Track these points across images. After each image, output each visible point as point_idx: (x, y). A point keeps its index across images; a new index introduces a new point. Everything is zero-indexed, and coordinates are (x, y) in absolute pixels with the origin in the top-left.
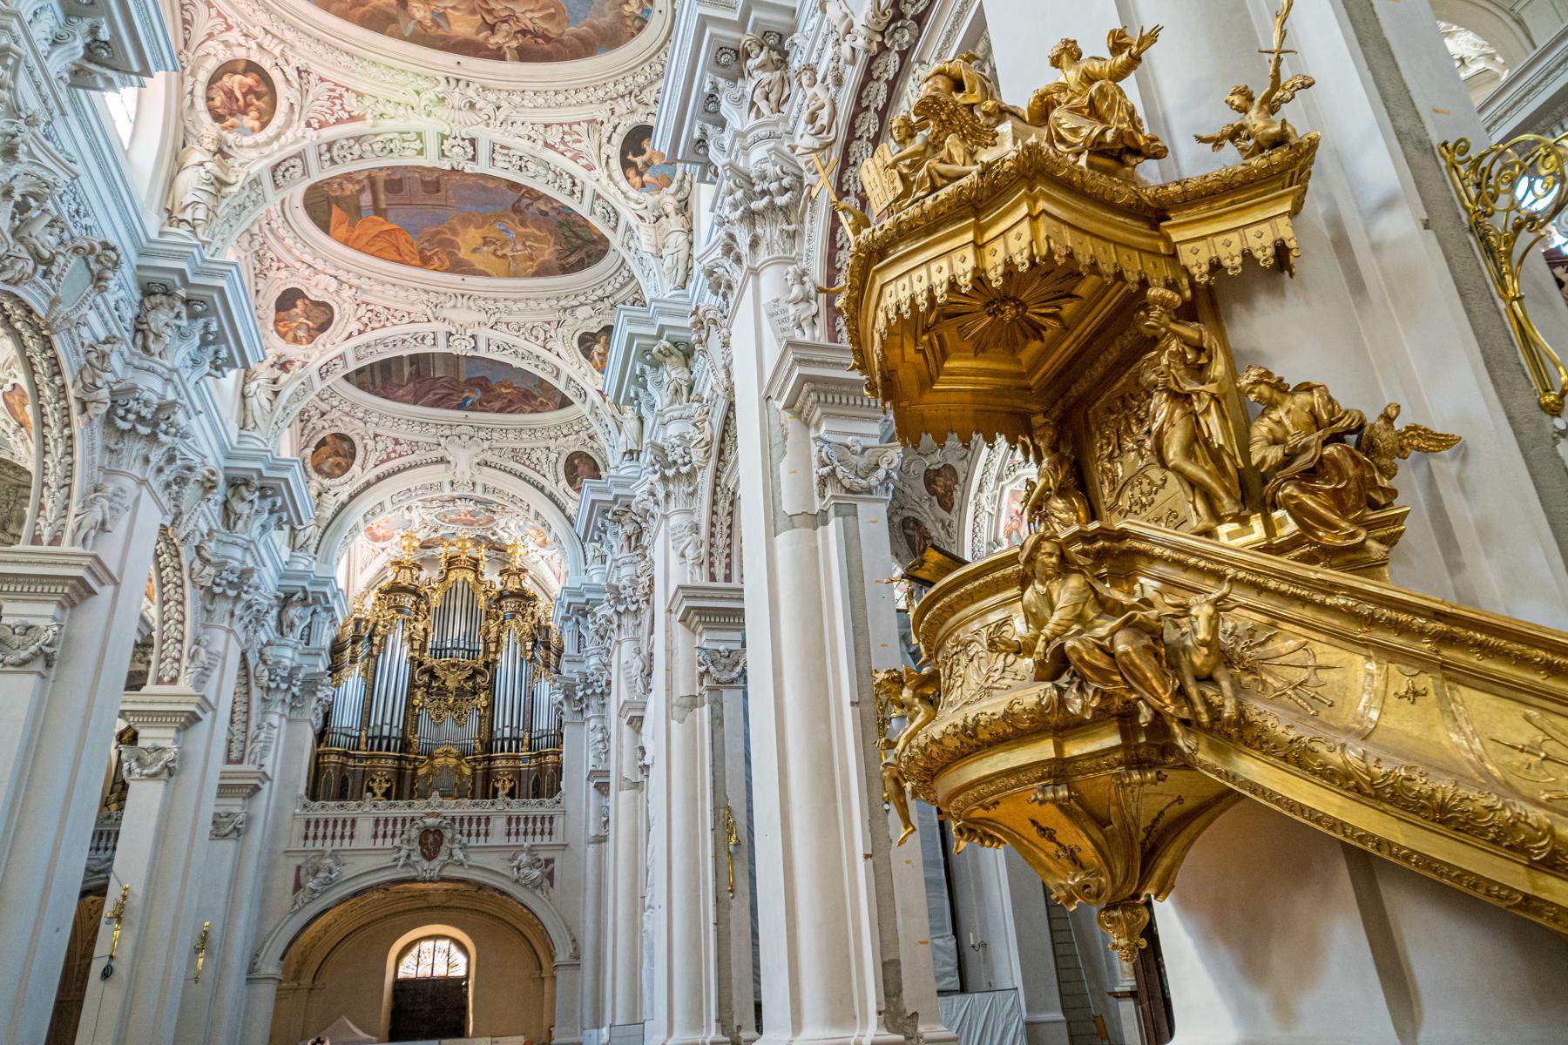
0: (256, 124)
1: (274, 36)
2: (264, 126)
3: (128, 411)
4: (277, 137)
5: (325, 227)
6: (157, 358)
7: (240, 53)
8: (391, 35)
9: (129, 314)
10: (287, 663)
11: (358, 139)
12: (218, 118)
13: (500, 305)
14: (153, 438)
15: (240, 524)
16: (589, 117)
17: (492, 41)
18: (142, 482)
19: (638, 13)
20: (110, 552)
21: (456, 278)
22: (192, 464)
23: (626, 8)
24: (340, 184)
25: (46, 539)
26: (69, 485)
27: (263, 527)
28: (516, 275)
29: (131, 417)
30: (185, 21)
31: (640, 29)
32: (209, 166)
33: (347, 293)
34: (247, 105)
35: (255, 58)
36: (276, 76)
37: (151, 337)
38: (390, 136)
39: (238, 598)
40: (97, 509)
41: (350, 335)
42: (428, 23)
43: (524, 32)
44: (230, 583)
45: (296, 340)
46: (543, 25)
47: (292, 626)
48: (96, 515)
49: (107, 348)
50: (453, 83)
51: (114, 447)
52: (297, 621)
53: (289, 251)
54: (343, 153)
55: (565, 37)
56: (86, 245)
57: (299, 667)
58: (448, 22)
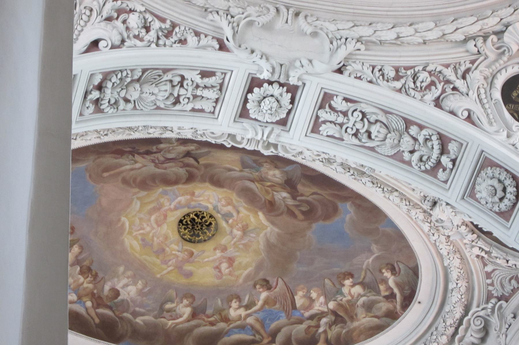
11: (398, 157)
38: (355, 141)
46: (121, 161)
54: (424, 151)
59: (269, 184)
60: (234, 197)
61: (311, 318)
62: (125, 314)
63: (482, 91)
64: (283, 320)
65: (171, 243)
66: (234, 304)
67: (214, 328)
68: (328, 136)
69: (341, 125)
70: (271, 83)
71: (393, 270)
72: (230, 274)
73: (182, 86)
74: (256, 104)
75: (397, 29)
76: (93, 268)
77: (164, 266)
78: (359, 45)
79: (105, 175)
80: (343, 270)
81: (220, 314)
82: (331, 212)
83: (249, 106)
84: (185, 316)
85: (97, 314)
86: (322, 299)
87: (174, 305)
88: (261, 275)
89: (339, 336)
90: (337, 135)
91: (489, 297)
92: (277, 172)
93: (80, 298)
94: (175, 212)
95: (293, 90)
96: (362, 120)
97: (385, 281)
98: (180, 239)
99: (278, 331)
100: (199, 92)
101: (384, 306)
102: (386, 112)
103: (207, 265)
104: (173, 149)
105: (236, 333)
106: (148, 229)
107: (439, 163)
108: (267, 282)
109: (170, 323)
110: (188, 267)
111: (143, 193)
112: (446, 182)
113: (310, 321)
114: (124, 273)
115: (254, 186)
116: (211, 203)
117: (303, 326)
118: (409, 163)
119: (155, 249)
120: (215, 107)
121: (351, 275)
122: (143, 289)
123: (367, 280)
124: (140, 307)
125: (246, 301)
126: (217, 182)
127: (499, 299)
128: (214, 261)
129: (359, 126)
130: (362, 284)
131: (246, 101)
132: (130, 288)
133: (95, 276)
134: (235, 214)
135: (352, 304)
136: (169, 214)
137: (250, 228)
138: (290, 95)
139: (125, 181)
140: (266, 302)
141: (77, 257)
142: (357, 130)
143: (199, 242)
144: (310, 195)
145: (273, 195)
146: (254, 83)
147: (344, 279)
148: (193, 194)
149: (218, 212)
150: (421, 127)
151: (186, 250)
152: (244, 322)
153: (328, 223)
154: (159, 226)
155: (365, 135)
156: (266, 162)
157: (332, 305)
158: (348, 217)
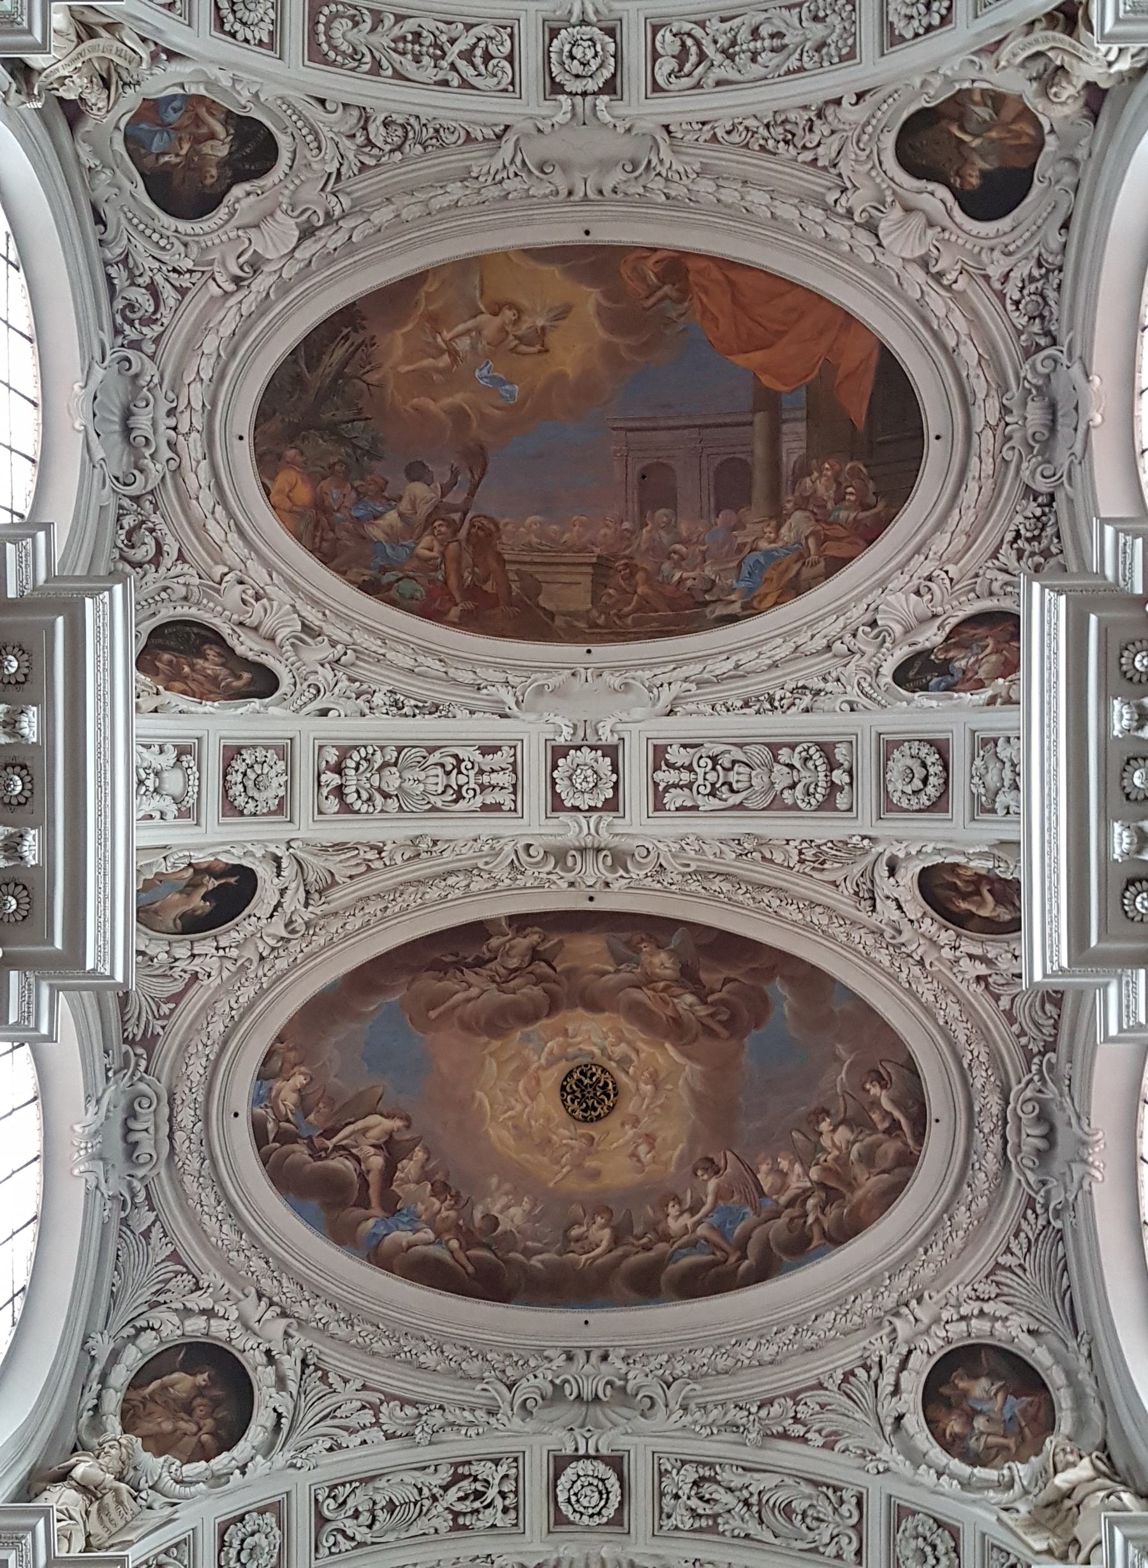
5: (889, 370)
11: (776, 804)
13: (495, 192)
16: (335, 894)
17: (536, 937)
19: (278, 1084)
21: (607, 234)
23: (299, 1080)
24: (840, 499)
28: (464, 266)
31: (270, 1055)
33: (859, 201)
35: (946, 937)
36: (915, 906)
38: (715, 803)
41: (860, 96)
42: (646, 948)
43: (481, 963)
45: (996, 99)
53: (975, 319)
55: (404, 979)
58: (613, 953)
59: (661, 985)
61: (790, 1204)
62: (512, 1255)
63: (865, 685)
64: (751, 1218)
65: (558, 1126)
66: (673, 1210)
67: (652, 1254)
68: (677, 809)
69: (689, 786)
70: (578, 748)
72: (654, 1160)
73: (460, 772)
74: (567, 782)
75: (735, 658)
76: (450, 1183)
77: (557, 1168)
78: (686, 686)
79: (433, 1014)
80: (812, 1107)
81: (655, 1230)
82: (761, 1007)
83: (558, 789)
84: (604, 1245)
85: (468, 1258)
86: (798, 1168)
87: (584, 1228)
88: (699, 1153)
89: (839, 1219)
90: (689, 804)
92: (662, 957)
93: (438, 1235)
94: (550, 1072)
95: (611, 752)
96: (714, 769)
97: (876, 1103)
98: (570, 1119)
99: (746, 1237)
100: (486, 779)
101: (890, 1148)
102: (740, 746)
104: (512, 947)
105: (685, 1255)
106: (519, 1107)
107: (833, 787)
108: (711, 1161)
109: (584, 1257)
110: (591, 1163)
111: (496, 1044)
112: (850, 810)
113: (789, 1210)
114: (498, 1188)
116: (595, 1044)
117: (783, 1220)
118: (795, 807)
119: (537, 1140)
120: (515, 801)
122: (533, 1209)
123: (850, 1113)
124: (533, 1240)
125: (688, 1202)
126: (593, 1005)
127: (1042, 1054)
128: (626, 1144)
129: (712, 777)
131: (554, 783)
132: (512, 1210)
133: (457, 1197)
134: (634, 1056)
135: (843, 1160)
136: (543, 1075)
137: (662, 1076)
138: (608, 760)
139: (466, 1026)
140: (718, 1196)
141: (423, 1167)
142: (713, 785)
143: (599, 1117)
144: (723, 985)
145: (674, 1005)
146: (559, 752)
147: (818, 1123)
148: (565, 1033)
149: (610, 1059)
150: (793, 747)
151: (583, 1135)
152: (693, 1236)
153: (761, 1031)
154: (532, 1099)
155: (725, 789)
156: (642, 940)
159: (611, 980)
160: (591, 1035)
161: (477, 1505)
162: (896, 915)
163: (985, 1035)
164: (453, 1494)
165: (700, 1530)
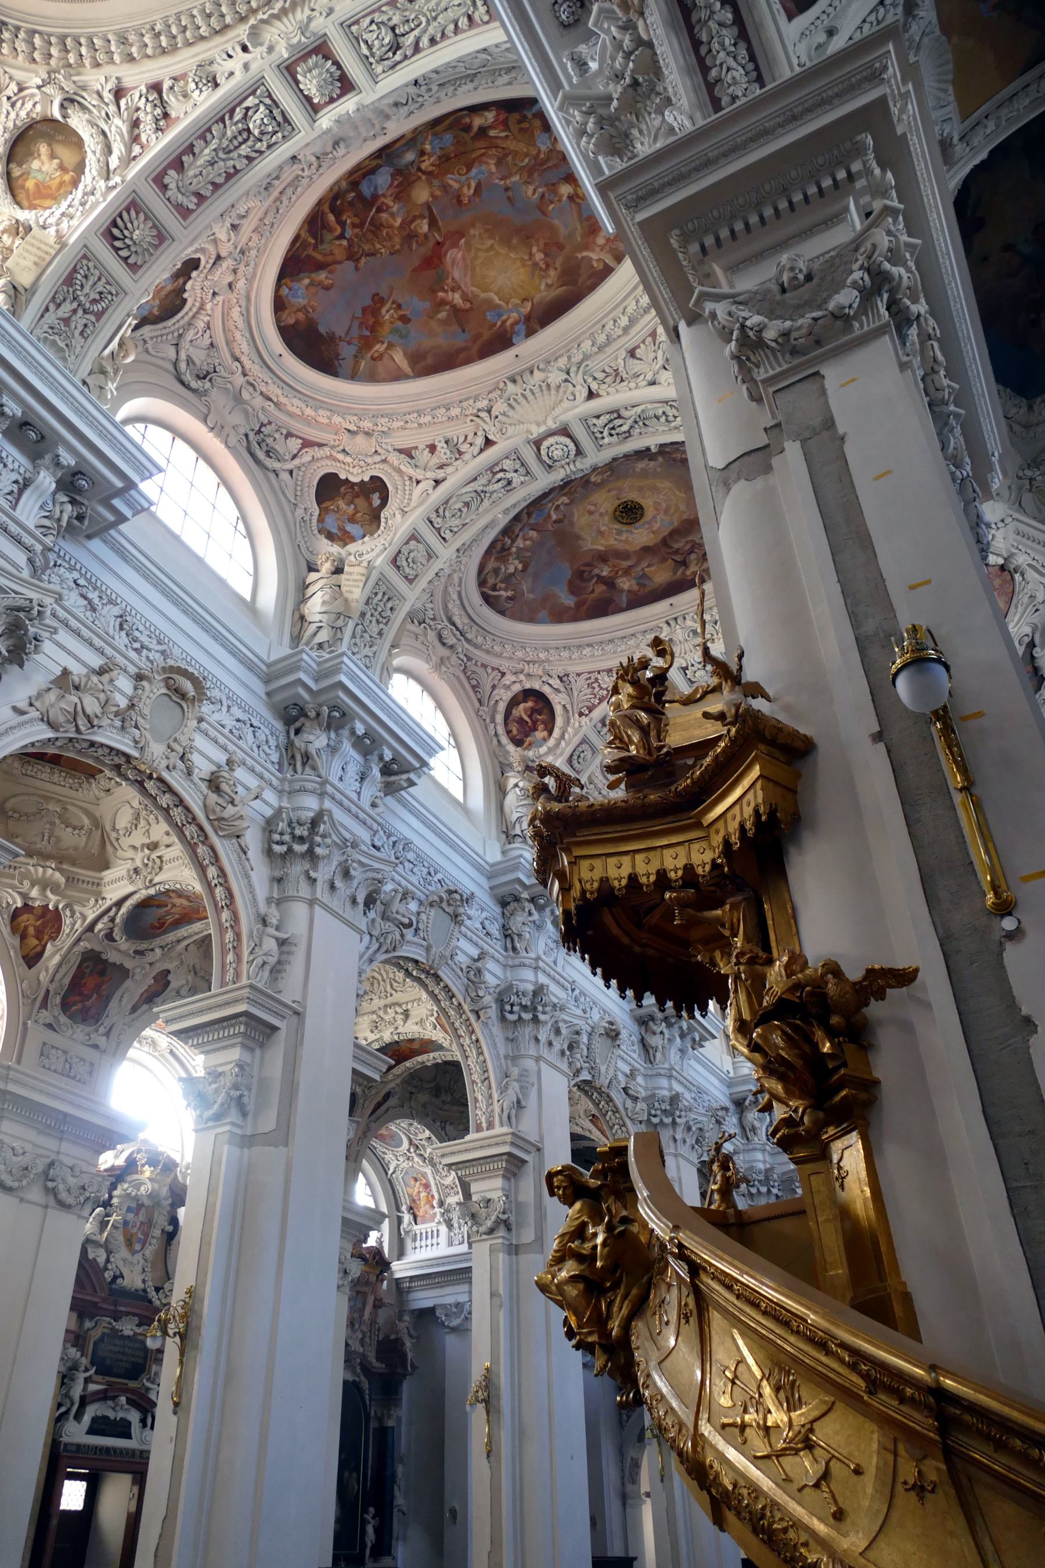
0: (545, 733)
1: (534, 662)
2: (550, 733)
3: (512, 1005)
4: (562, 737)
6: (524, 954)
7: (517, 688)
8: (613, 613)
9: (495, 929)
10: (761, 1166)
12: (518, 743)
14: (535, 1020)
15: (659, 1055)
17: (688, 573)
18: (538, 1059)
20: (527, 1127)
22: (577, 1028)
25: (484, 1125)
26: (487, 1078)
27: (681, 1050)
29: (516, 1008)
30: (473, 687)
32: (521, 784)
34: (535, 723)
35: (528, 686)
36: (546, 690)
37: (516, 938)
39: (674, 1123)
40: (510, 1091)
42: (635, 588)
44: (665, 1111)
47: (754, 1129)
48: (511, 1096)
49: (479, 964)
50: (672, 623)
51: (511, 1036)
52: (757, 1124)
56: (436, 898)
57: (772, 1169)
58: (649, 579)
60: (628, 547)
64: (532, 521)
71: (509, 598)
82: (573, 589)
91: (469, 659)
97: (506, 590)
101: (491, 581)
103: (605, 502)
110: (614, 493)
111: (685, 517)
115: (625, 564)
121: (524, 570)
126: (646, 550)
130: (513, 574)
140: (549, 516)
157: (514, 550)
158: (562, 595)
159: (644, 564)
160: (640, 536)
161: (611, 426)
162: (551, 682)
163: (488, 652)
164: (625, 428)
165: (497, 464)
